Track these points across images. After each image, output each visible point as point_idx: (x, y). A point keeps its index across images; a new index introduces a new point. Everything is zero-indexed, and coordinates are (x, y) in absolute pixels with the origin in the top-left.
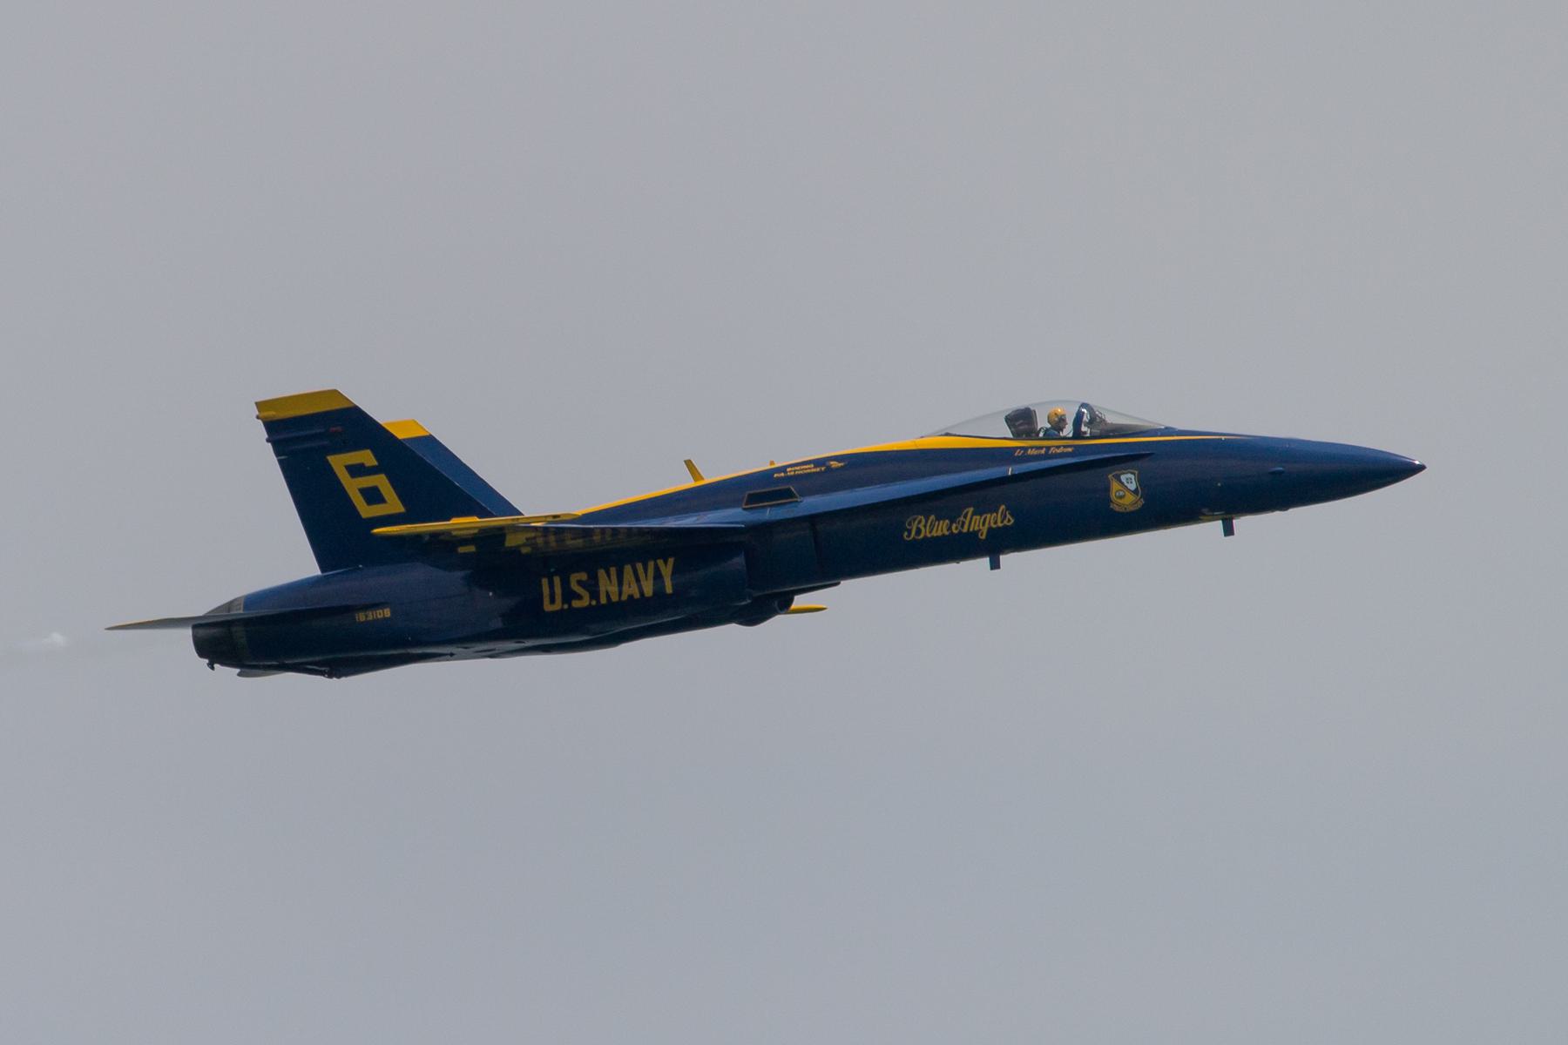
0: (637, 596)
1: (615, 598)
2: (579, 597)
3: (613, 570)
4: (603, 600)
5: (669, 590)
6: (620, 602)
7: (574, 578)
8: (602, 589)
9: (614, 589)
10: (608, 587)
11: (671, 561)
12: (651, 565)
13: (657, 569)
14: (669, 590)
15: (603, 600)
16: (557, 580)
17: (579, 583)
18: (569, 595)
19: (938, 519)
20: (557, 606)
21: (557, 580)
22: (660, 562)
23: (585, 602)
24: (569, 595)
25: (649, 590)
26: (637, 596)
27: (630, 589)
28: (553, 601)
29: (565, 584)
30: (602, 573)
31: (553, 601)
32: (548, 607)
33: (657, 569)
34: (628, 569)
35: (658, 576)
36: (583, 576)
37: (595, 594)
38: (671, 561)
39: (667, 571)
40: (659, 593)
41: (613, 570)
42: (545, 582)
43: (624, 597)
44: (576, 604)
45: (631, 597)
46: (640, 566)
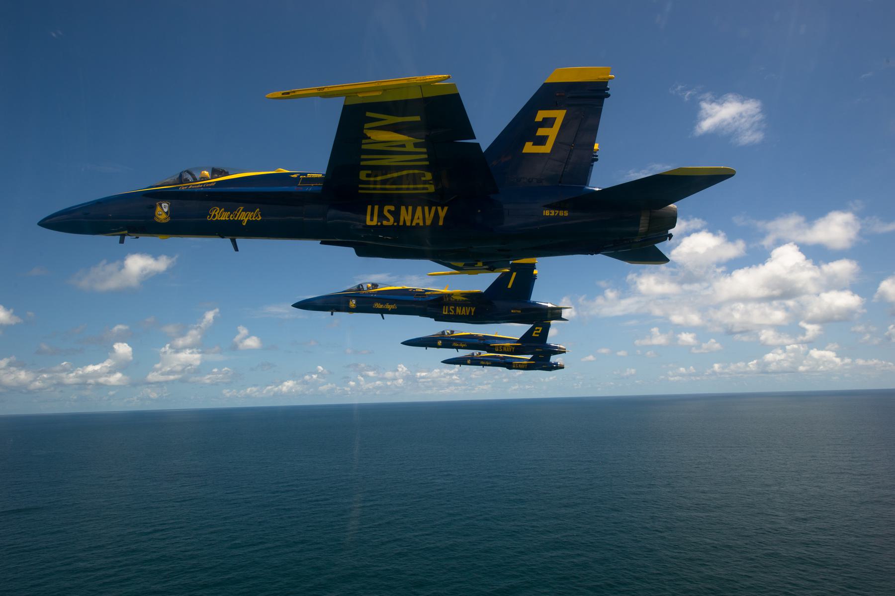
1: (408, 224)
2: (388, 220)
3: (410, 208)
4: (401, 223)
5: (441, 223)
6: (411, 227)
7: (386, 208)
9: (408, 218)
10: (405, 216)
11: (446, 208)
12: (434, 209)
13: (436, 211)
14: (441, 223)
15: (401, 223)
16: (376, 207)
17: (389, 211)
20: (374, 223)
21: (376, 207)
22: (439, 208)
25: (428, 222)
26: (421, 224)
27: (418, 220)
28: (372, 220)
30: (403, 208)
31: (372, 220)
32: (369, 223)
34: (419, 209)
36: (392, 208)
37: (397, 220)
38: (446, 208)
41: (410, 208)
42: (369, 207)
43: (414, 224)
44: (385, 223)
46: (426, 208)
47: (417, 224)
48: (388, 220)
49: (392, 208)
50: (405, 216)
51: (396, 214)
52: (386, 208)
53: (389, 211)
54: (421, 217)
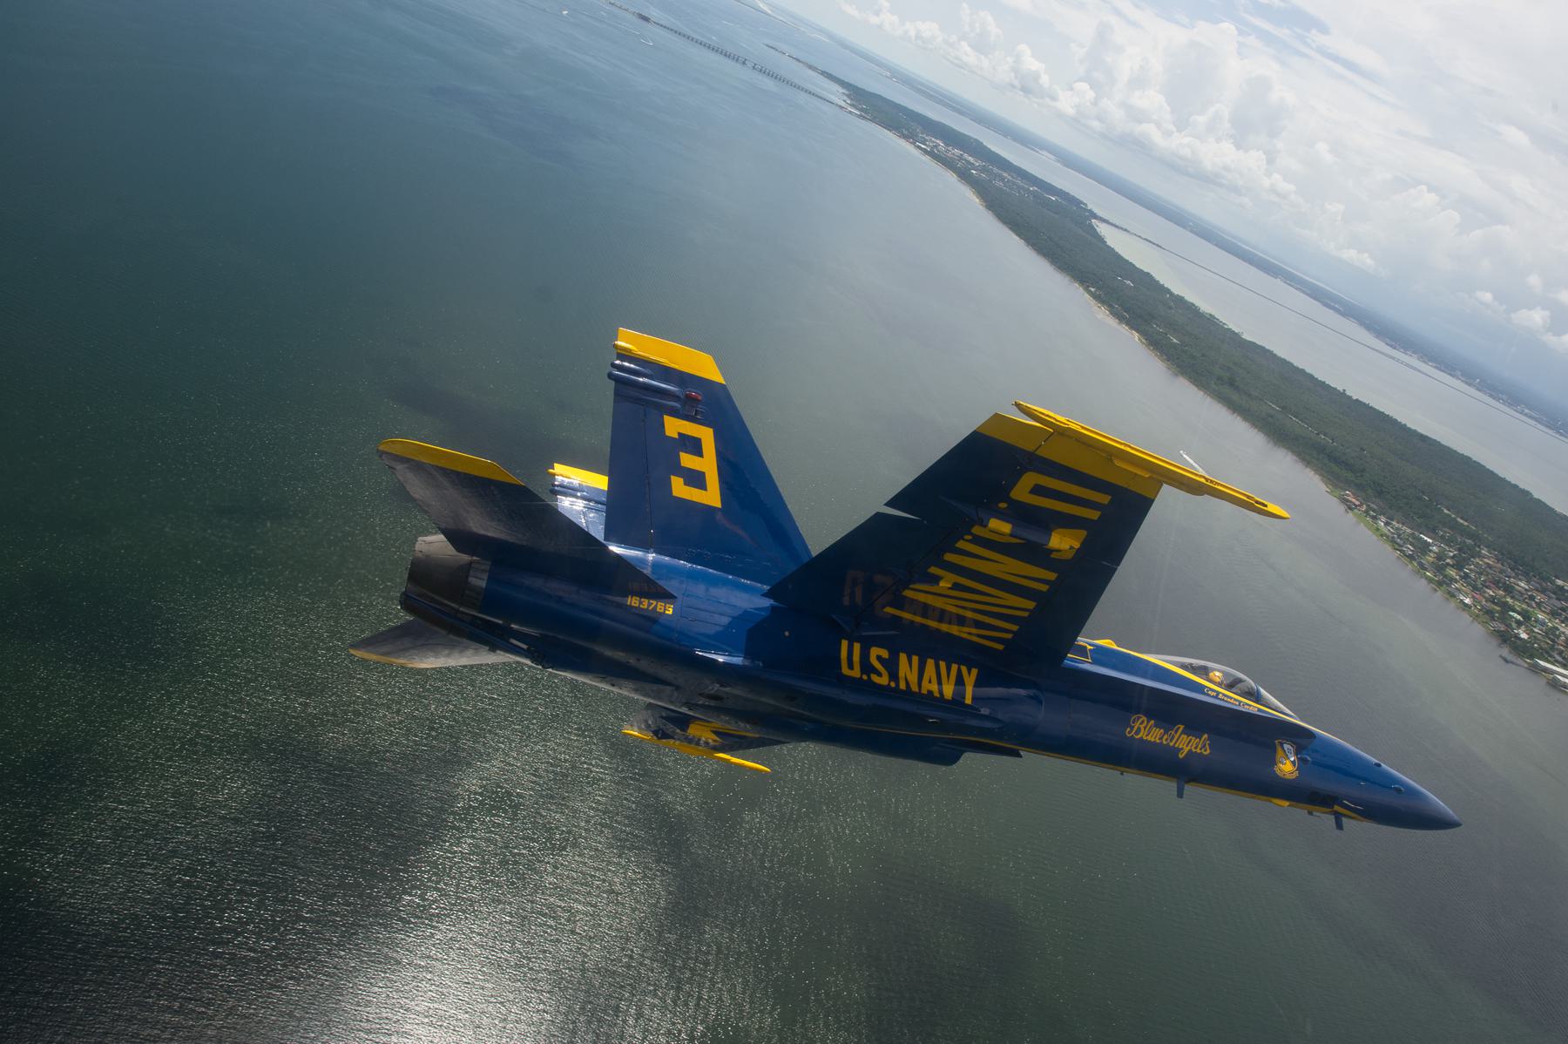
1: (915, 688)
5: (968, 701)
7: (875, 652)
8: (901, 674)
9: (913, 678)
10: (907, 669)
11: (975, 671)
12: (954, 667)
13: (959, 671)
16: (857, 647)
17: (879, 658)
18: (867, 667)
19: (1156, 726)
20: (856, 673)
21: (857, 647)
22: (964, 669)
23: (883, 680)
24: (867, 667)
26: (937, 694)
28: (851, 666)
30: (903, 657)
31: (851, 666)
32: (845, 671)
33: (959, 671)
34: (930, 663)
35: (960, 681)
36: (885, 654)
37: (894, 676)
39: (970, 680)
40: (958, 700)
41: (915, 659)
42: (845, 644)
43: (924, 691)
44: (875, 678)
45: (930, 692)
46: (942, 664)
48: (880, 675)
49: (885, 654)
51: (892, 666)
52: (875, 652)
53: (879, 658)
54: (934, 680)
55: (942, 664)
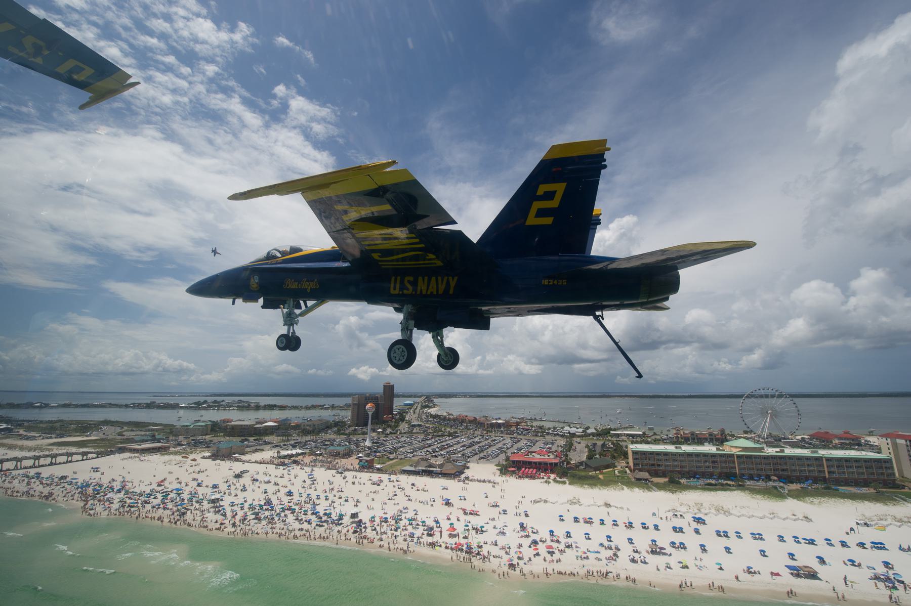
0: (435, 293)
1: (424, 292)
2: (408, 289)
3: (426, 278)
5: (451, 292)
8: (419, 288)
9: (424, 288)
11: (456, 278)
12: (446, 278)
14: (451, 292)
15: (418, 293)
16: (399, 278)
17: (409, 281)
20: (397, 292)
21: (399, 278)
22: (450, 278)
26: (435, 293)
27: (433, 289)
28: (395, 289)
29: (402, 282)
30: (420, 279)
31: (395, 289)
32: (392, 292)
34: (434, 279)
36: (411, 279)
39: (453, 284)
41: (426, 278)
43: (429, 293)
44: (405, 292)
45: (432, 293)
47: (432, 293)
48: (408, 289)
49: (411, 279)
50: (422, 286)
51: (414, 284)
52: (407, 278)
53: (409, 281)
55: (440, 278)
